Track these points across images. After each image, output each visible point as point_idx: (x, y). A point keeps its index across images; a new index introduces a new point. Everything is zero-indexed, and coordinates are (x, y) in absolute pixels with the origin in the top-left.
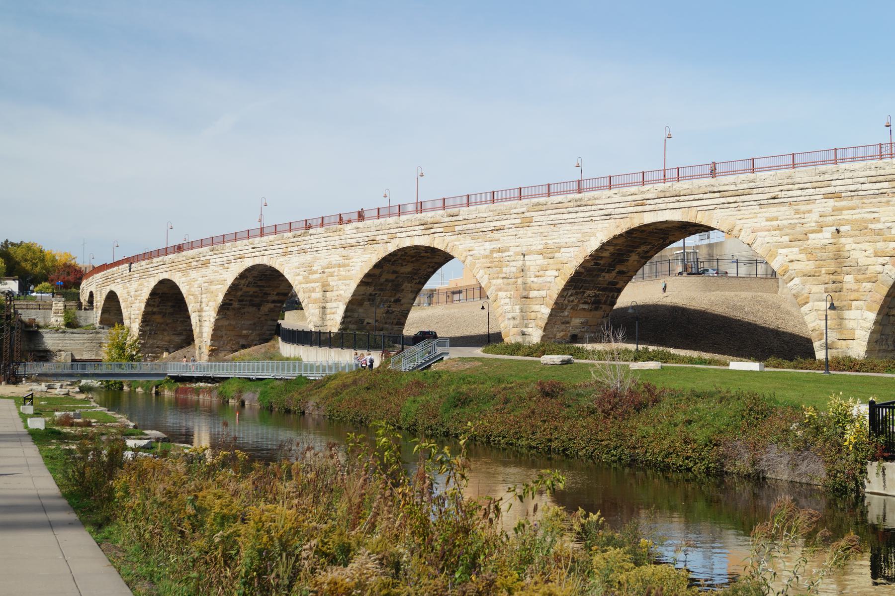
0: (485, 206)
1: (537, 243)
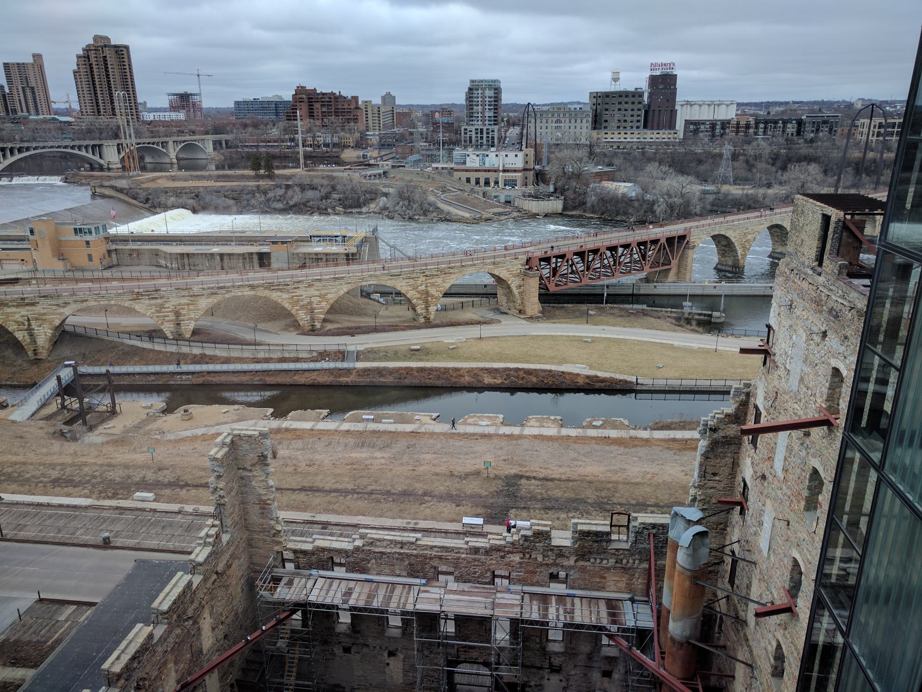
1: (317, 293)
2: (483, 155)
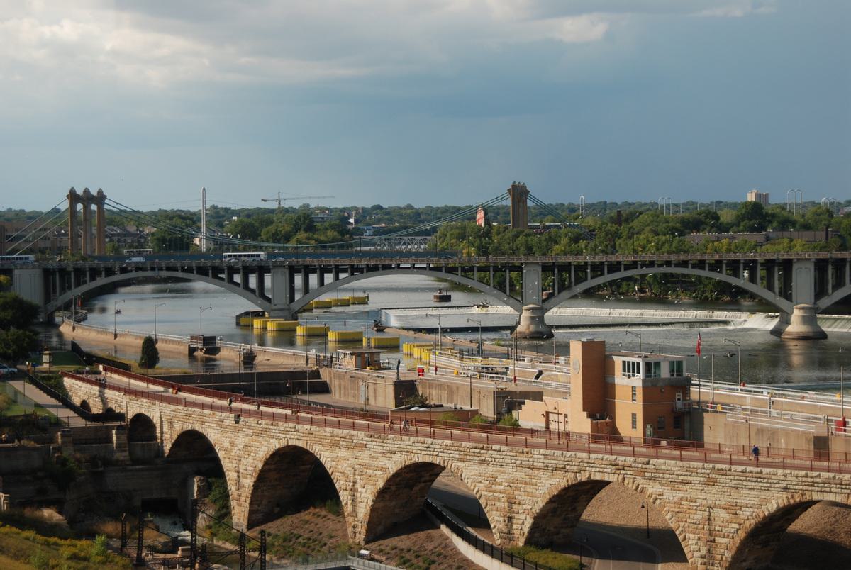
0: (673, 462)
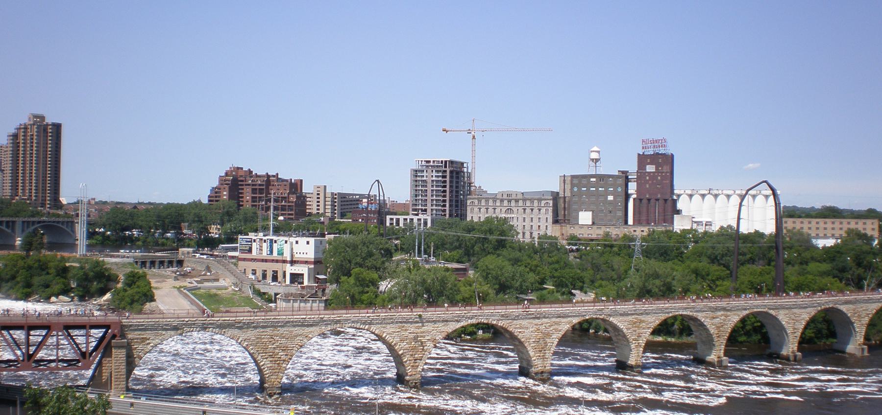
2: (271, 240)
